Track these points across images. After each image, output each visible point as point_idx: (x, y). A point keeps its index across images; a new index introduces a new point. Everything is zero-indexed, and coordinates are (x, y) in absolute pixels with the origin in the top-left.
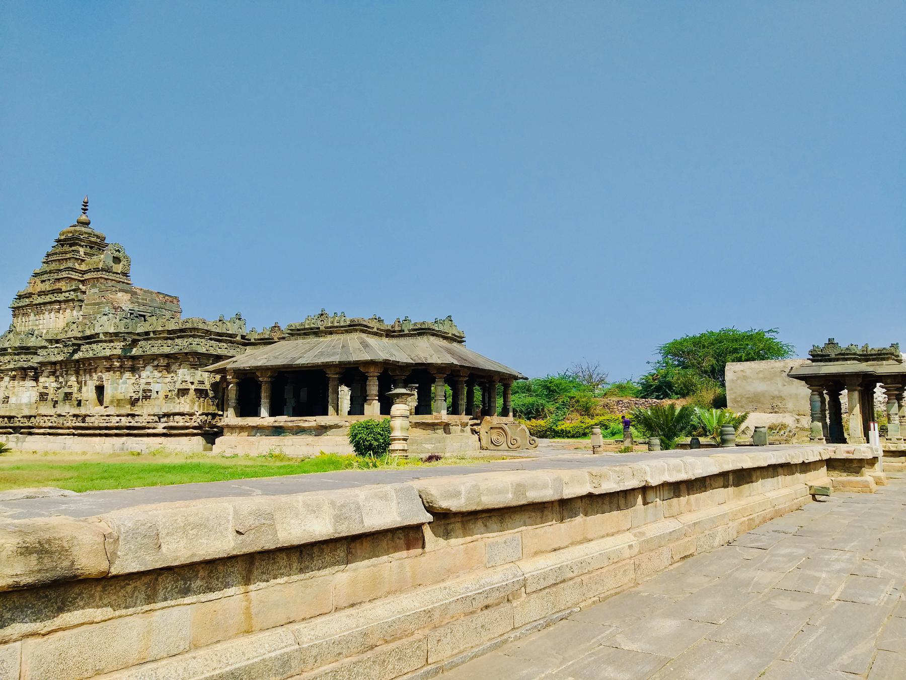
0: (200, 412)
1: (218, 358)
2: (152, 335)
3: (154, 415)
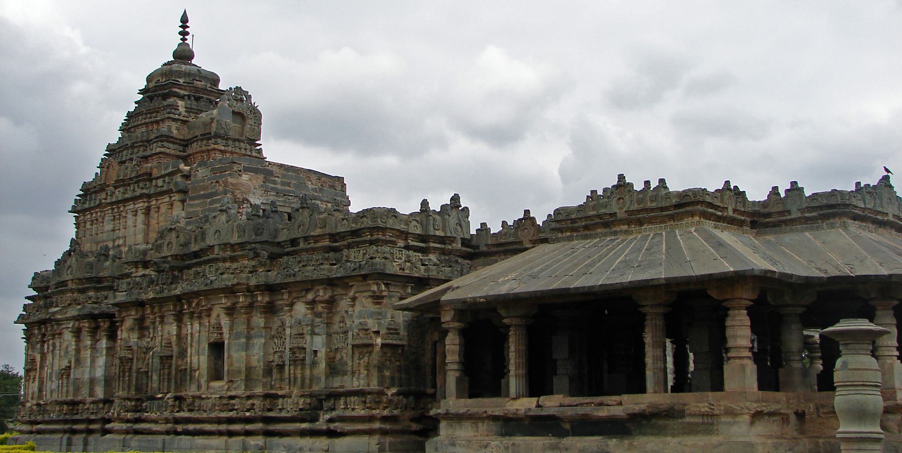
1: (422, 283)
2: (302, 245)
3: (311, 396)
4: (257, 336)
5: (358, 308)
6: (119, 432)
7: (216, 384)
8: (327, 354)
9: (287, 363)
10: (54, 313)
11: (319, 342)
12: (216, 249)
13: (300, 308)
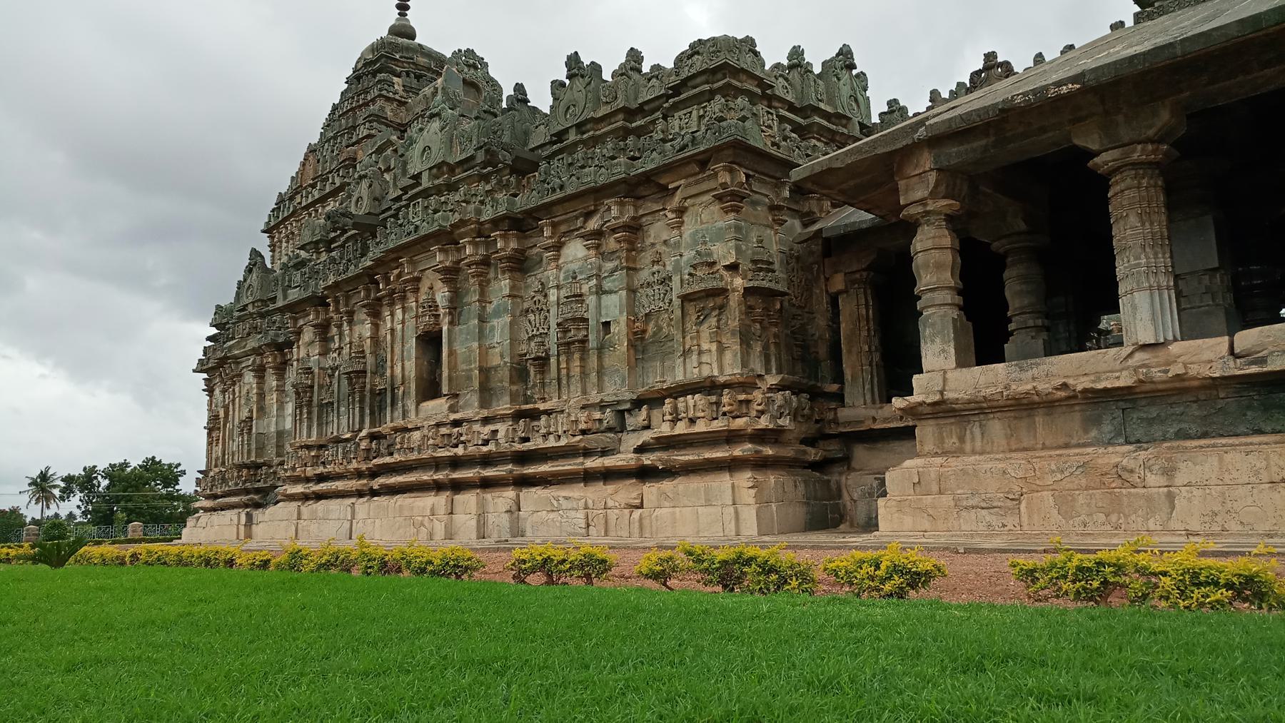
0: (772, 380)
3: (602, 406)
4: (497, 314)
5: (688, 229)
6: (292, 498)
7: (430, 406)
8: (630, 323)
9: (554, 351)
10: (230, 348)
11: (613, 306)
12: (425, 176)
13: (576, 251)
